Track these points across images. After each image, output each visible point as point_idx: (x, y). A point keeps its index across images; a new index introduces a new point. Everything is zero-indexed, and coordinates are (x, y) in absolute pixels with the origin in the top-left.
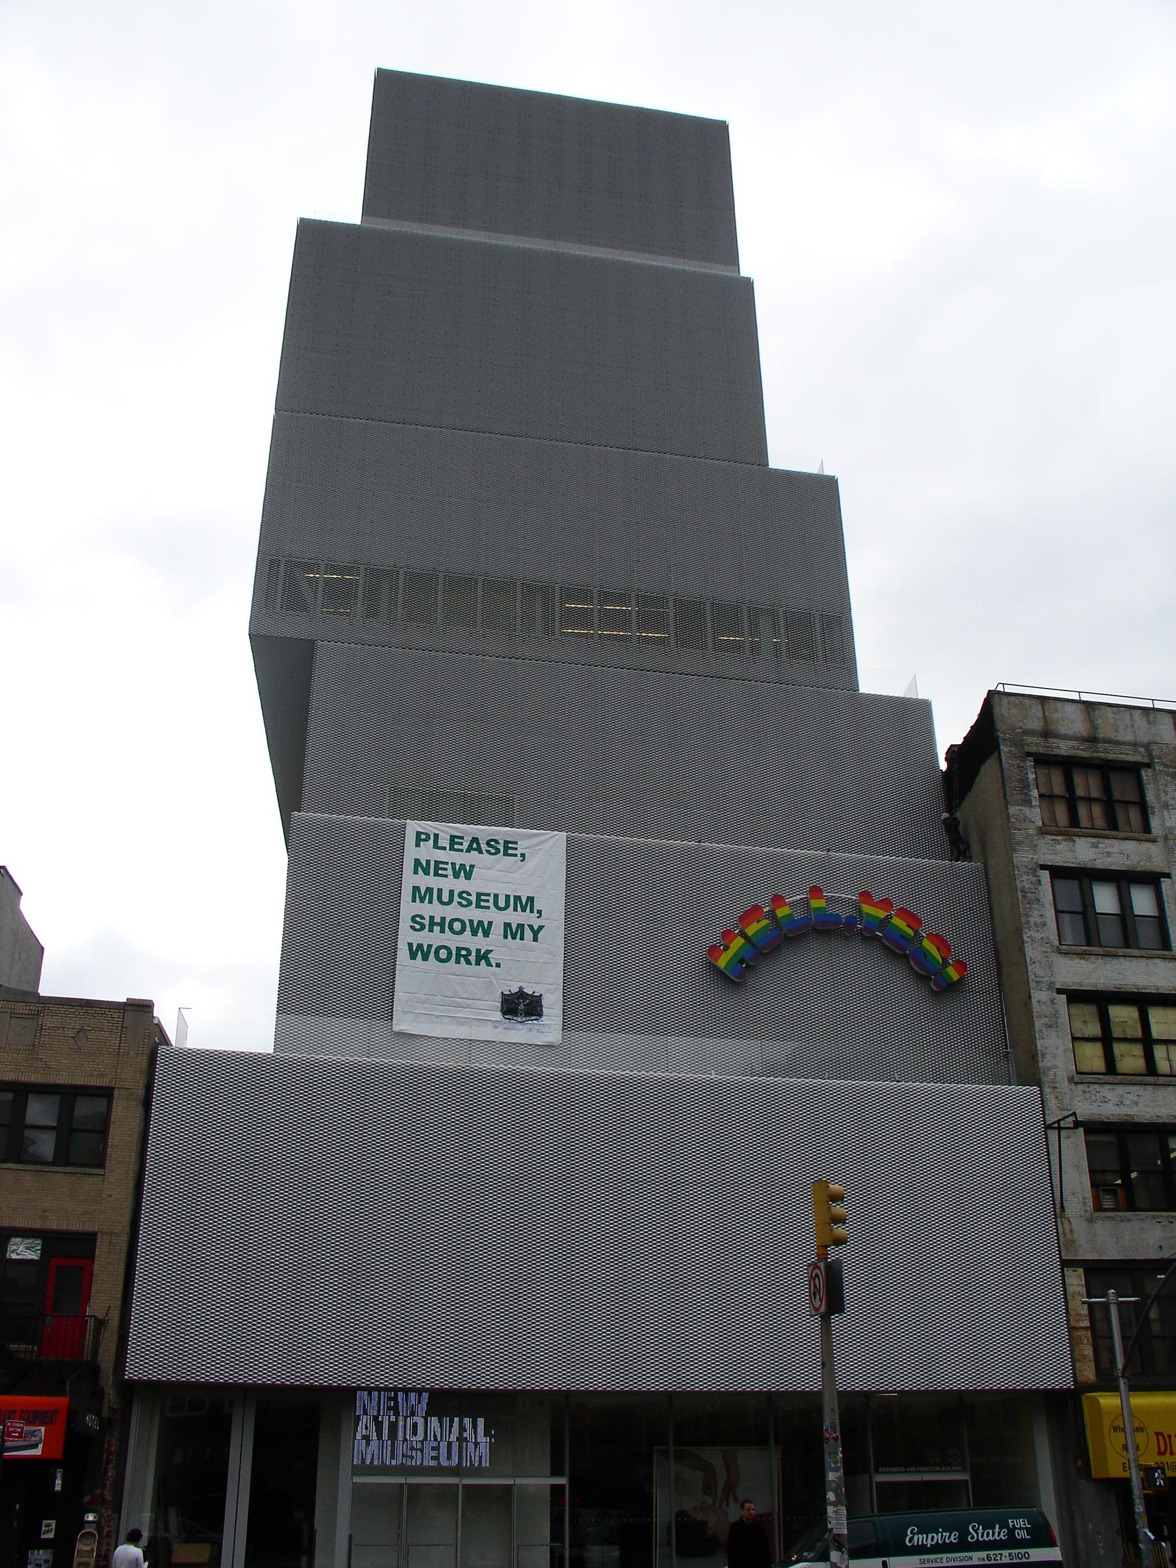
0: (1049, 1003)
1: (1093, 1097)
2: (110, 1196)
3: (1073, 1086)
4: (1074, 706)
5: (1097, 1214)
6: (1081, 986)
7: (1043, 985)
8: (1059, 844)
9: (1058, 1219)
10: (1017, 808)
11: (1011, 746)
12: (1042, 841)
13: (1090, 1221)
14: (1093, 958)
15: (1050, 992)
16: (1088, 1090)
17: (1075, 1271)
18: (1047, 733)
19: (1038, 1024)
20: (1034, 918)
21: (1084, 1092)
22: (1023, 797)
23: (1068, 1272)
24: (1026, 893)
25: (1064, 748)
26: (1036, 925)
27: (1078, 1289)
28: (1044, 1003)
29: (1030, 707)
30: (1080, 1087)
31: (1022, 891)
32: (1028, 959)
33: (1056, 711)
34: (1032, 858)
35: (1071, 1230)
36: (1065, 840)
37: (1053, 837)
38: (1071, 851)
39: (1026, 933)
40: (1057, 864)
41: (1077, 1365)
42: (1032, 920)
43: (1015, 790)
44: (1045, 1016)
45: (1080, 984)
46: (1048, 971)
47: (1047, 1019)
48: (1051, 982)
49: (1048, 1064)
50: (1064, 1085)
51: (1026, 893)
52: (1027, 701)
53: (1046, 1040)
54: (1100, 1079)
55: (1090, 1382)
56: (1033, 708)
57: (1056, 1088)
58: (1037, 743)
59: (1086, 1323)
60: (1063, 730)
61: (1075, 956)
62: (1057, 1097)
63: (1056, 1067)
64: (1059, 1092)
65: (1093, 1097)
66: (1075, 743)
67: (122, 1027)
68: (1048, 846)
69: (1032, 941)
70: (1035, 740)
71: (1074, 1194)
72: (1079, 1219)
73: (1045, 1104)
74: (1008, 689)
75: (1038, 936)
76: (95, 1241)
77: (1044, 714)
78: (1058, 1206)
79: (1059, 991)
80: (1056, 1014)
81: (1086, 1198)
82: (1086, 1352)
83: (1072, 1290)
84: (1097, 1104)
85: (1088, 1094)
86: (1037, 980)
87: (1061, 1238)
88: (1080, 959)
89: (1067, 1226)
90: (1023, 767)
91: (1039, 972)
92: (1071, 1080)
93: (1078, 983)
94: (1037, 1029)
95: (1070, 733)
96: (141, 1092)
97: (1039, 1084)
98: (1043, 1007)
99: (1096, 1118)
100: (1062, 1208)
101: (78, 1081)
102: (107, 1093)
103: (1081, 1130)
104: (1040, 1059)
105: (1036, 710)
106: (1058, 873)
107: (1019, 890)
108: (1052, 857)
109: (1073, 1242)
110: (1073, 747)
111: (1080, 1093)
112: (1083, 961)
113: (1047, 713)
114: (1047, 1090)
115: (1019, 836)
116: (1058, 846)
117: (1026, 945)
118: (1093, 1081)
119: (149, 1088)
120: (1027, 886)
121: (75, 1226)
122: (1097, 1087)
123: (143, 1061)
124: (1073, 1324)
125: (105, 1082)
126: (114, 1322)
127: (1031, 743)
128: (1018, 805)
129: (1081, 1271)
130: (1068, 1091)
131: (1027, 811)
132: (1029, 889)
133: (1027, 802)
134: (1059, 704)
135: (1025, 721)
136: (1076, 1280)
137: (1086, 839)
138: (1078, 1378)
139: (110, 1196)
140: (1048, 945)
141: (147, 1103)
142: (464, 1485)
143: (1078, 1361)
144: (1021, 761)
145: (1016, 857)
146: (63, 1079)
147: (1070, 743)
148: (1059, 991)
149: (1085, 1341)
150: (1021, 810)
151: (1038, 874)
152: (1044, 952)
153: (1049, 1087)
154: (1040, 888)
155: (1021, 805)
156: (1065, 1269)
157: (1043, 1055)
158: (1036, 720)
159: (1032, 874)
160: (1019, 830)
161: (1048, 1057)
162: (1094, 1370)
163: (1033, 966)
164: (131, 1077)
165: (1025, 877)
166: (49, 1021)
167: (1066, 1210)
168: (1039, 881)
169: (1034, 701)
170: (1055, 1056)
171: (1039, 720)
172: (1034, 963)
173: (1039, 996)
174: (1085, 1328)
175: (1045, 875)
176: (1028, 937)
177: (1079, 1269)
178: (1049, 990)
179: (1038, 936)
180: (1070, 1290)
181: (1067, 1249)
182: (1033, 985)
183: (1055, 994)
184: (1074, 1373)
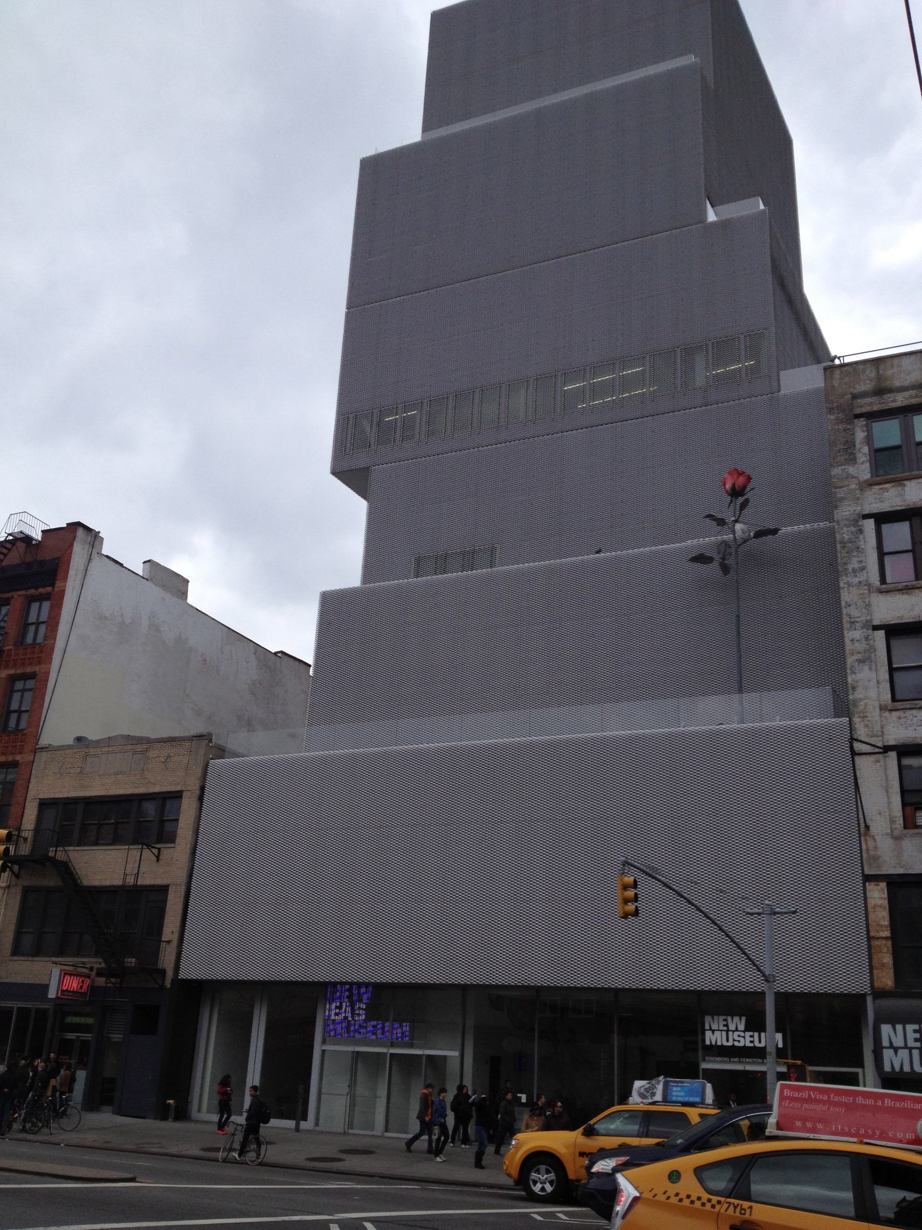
0: (864, 642)
1: (909, 722)
2: (177, 860)
3: (887, 714)
4: (913, 358)
5: (906, 831)
6: (902, 619)
7: (858, 624)
8: (888, 492)
9: (862, 837)
10: (840, 468)
11: (838, 413)
12: (870, 493)
13: (897, 838)
14: (917, 591)
15: (865, 630)
16: (904, 715)
17: (877, 885)
18: (880, 392)
19: (850, 660)
20: (854, 564)
21: (899, 718)
22: (847, 457)
23: (870, 886)
24: (845, 543)
25: (900, 400)
26: (854, 571)
27: (879, 902)
28: (858, 641)
29: (864, 371)
30: (895, 714)
31: (841, 543)
32: (843, 604)
33: (892, 366)
34: (855, 511)
35: (876, 848)
36: (893, 486)
37: (881, 487)
38: (901, 495)
39: (843, 580)
40: (883, 510)
41: (875, 972)
42: (850, 567)
43: (839, 452)
44: (860, 653)
45: (901, 618)
46: (864, 610)
47: (860, 655)
48: (867, 621)
49: (860, 696)
50: (875, 714)
51: (845, 543)
52: (861, 367)
53: (858, 675)
54: (916, 705)
55: (888, 988)
56: (867, 371)
57: (866, 717)
58: (871, 403)
59: (887, 933)
60: (897, 383)
61: (896, 592)
62: (867, 726)
63: (866, 698)
64: (869, 721)
65: (909, 722)
66: (913, 392)
67: (191, 751)
68: (875, 496)
69: (849, 586)
70: (869, 400)
71: (880, 814)
72: (885, 836)
73: (853, 733)
74: (847, 360)
75: (856, 580)
76: (168, 890)
77: (878, 372)
78: (862, 825)
79: (876, 628)
80: (872, 649)
81: (895, 817)
82: (885, 961)
83: (874, 903)
84: (912, 728)
85: (904, 720)
86: (852, 620)
87: (865, 855)
88: (903, 594)
89: (871, 843)
90: (849, 429)
91: (854, 612)
92: (883, 708)
93: (898, 617)
94: (848, 666)
95: (906, 384)
96: (197, 792)
97: (849, 715)
98: (857, 644)
99: (909, 741)
100: (867, 827)
101: (165, 789)
102: (177, 796)
103: (893, 755)
104: (851, 692)
105: (871, 373)
106: (882, 519)
107: (838, 543)
108: (879, 505)
109: (876, 858)
110: (911, 397)
111: (895, 719)
112: (906, 597)
113: (881, 372)
114: (856, 720)
115: (840, 493)
116: (886, 494)
117: (841, 591)
118: (908, 706)
119: (203, 789)
120: (846, 537)
121: (158, 882)
122: (914, 712)
123: (199, 771)
124: (872, 934)
125: (178, 788)
126: (175, 943)
127: (866, 404)
128: (840, 465)
129: (883, 885)
130: (877, 718)
131: (851, 470)
132: (850, 539)
133: (853, 460)
134: (895, 361)
135: (857, 386)
136: (878, 894)
137: (916, 481)
138: (876, 985)
139: (177, 860)
140: (866, 587)
141: (201, 799)
142: (392, 1054)
143: (877, 969)
144: (848, 424)
145: (838, 513)
146: (157, 789)
147: (906, 394)
148: (876, 628)
149: (885, 950)
150: (845, 469)
151: (860, 523)
152: (860, 594)
153: (859, 717)
154: (861, 537)
155: (845, 465)
156: (867, 884)
157: (854, 688)
158: (868, 382)
159: (853, 525)
160: (841, 487)
161: (859, 690)
162: (893, 978)
163: (849, 609)
164: (193, 785)
165: (845, 529)
166: (152, 754)
167: (872, 829)
168: (861, 531)
169: (869, 365)
170: (866, 688)
171: (871, 381)
172: (850, 606)
173: (853, 636)
174: (886, 938)
175: (870, 524)
176: (845, 583)
177: (881, 884)
178: (862, 628)
179: (856, 580)
180: (871, 902)
181: (870, 865)
182: (846, 625)
183: (870, 631)
184: (872, 980)
